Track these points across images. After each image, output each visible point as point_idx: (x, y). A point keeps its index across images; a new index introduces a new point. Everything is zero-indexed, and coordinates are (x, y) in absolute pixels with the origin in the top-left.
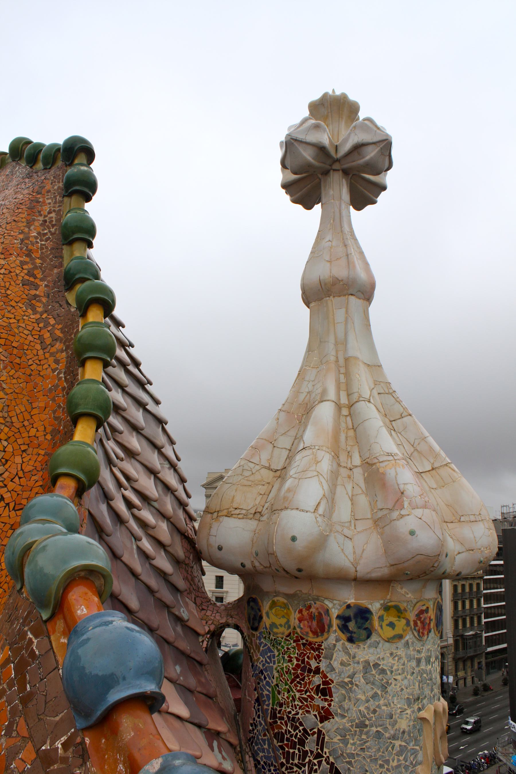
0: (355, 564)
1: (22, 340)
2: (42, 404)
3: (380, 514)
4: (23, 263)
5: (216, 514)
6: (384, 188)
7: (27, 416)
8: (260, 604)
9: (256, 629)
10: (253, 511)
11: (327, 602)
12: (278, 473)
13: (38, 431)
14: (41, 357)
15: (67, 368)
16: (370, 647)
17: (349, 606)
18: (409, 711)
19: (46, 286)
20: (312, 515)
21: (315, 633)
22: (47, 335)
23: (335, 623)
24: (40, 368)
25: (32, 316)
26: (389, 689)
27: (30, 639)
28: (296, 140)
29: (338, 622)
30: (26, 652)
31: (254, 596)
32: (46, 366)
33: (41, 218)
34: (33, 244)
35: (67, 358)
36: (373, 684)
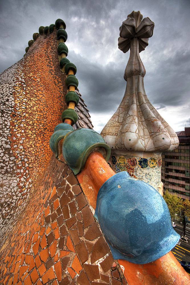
0: (145, 147)
1: (49, 82)
2: (56, 101)
3: (152, 134)
4: (47, 60)
5: (104, 135)
6: (147, 45)
7: (52, 105)
8: (116, 158)
9: (115, 164)
10: (115, 133)
11: (135, 157)
12: (121, 123)
15: (63, 90)
16: (147, 169)
17: (142, 159)
18: (156, 186)
20: (135, 133)
21: (132, 166)
23: (138, 163)
24: (55, 91)
26: (152, 180)
27: (68, 185)
28: (126, 25)
29: (139, 162)
30: (67, 192)
31: (114, 156)
32: (57, 90)
33: (51, 47)
34: (49, 54)
35: (63, 87)
36: (148, 179)
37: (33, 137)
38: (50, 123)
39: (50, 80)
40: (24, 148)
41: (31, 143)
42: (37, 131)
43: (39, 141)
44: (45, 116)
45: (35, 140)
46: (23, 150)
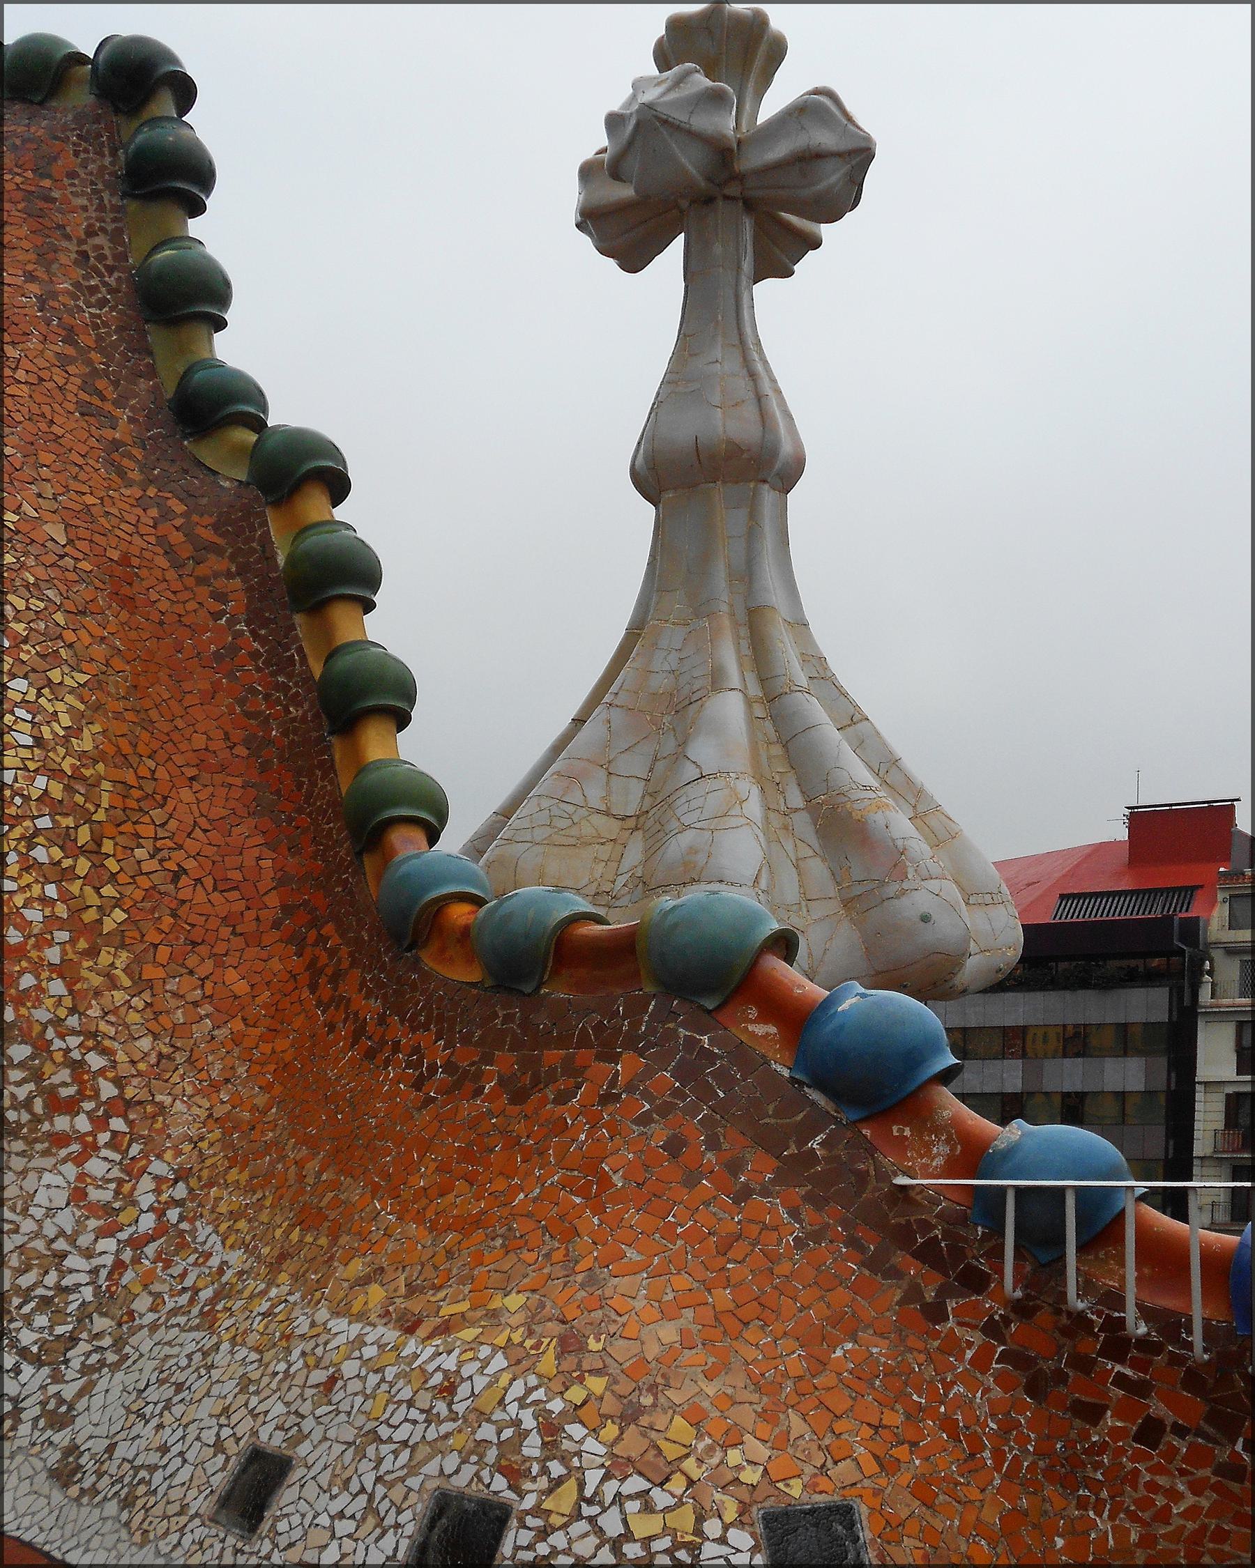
2: (206, 685)
13: (209, 738)
14: (177, 586)
19: (131, 420)
22: (177, 537)
25: (127, 492)
32: (192, 605)
37: (108, 925)
38: (198, 833)
39: (130, 529)
40: (71, 992)
41: (105, 959)
42: (128, 890)
43: (156, 946)
44: (149, 787)
45: (128, 941)
46: (68, 1002)
